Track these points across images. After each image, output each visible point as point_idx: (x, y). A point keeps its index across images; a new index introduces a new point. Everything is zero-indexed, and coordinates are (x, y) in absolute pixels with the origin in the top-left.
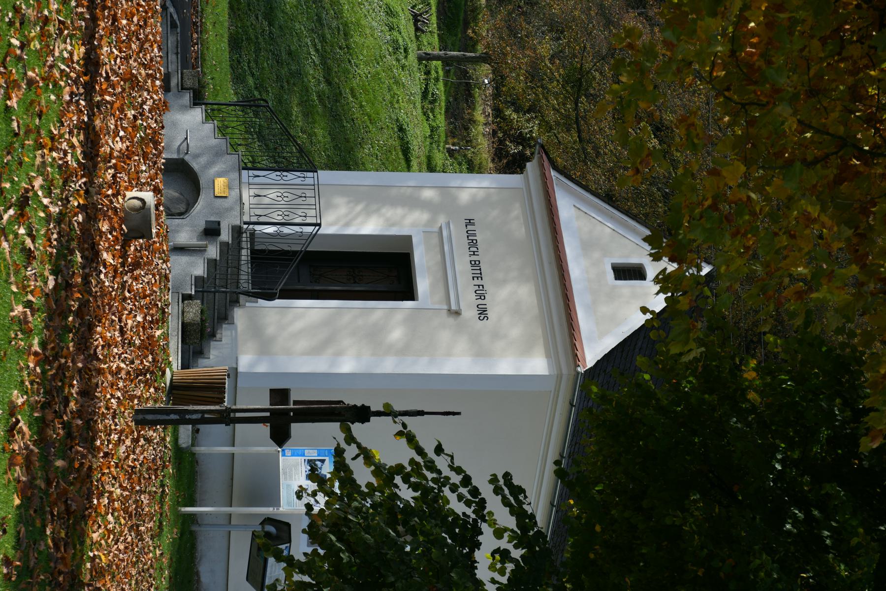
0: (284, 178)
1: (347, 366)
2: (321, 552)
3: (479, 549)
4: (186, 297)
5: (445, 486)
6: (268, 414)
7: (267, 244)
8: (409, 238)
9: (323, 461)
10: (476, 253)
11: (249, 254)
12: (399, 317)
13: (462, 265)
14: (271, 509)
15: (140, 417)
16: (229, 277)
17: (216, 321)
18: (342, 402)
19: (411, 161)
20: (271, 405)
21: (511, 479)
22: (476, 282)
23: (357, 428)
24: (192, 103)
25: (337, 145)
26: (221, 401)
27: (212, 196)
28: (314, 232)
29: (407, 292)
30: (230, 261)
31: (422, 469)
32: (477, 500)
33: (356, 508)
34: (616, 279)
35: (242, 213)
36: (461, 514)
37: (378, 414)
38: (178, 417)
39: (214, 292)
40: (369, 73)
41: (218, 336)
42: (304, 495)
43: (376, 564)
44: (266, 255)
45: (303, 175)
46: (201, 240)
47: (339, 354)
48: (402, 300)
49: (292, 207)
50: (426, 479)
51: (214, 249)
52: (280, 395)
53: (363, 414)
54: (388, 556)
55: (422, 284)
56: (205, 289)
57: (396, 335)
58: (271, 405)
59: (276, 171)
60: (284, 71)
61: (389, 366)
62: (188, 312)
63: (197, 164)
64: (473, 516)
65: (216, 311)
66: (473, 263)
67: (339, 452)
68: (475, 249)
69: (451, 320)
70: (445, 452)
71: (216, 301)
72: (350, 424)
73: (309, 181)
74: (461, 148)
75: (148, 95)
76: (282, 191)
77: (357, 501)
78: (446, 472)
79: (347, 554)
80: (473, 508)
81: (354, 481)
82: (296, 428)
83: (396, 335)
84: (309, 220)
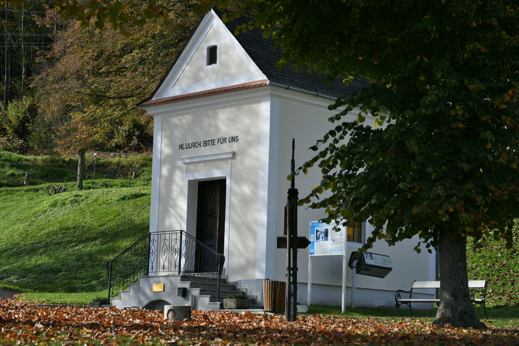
0: (154, 252)
1: (263, 217)
2: (370, 217)
3: (371, 127)
4: (222, 307)
5: (335, 146)
6: (292, 249)
7: (192, 261)
8: (190, 182)
9: (317, 231)
11: (197, 273)
12: (235, 188)
13: (206, 151)
14: (344, 260)
15: (292, 318)
16: (211, 284)
17: (235, 292)
18: (285, 207)
19: (142, 193)
20: (286, 248)
21: (332, 105)
22: (216, 143)
23: (301, 196)
24: (109, 305)
25: (132, 234)
26: (283, 284)
27: (163, 293)
28: (185, 234)
29: (221, 183)
30: (202, 283)
31: (325, 160)
32: (343, 127)
33: (346, 194)
34: (216, 63)
35: (174, 276)
36: (351, 137)
37: (293, 184)
38: (293, 297)
39: (219, 292)
40: (90, 216)
41: (244, 291)
42: (338, 227)
43: (378, 184)
44: (198, 261)
45: (152, 241)
46: (189, 299)
47: (256, 222)
48: (226, 185)
49: (171, 249)
50: (331, 157)
51: (194, 291)
52: (281, 243)
53: (293, 193)
54: (374, 177)
55: (217, 174)
56: (217, 296)
57: (246, 189)
58: (286, 248)
59: (149, 256)
60: (88, 263)
61: (264, 194)
62: (230, 305)
63: (144, 302)
64: (352, 130)
65: (230, 291)
66: (205, 145)
67: (314, 206)
68: (197, 144)
69: (238, 157)
70: (315, 145)
71: (224, 291)
72: (299, 200)
73: (156, 237)
74: (134, 170)
75: (107, 313)
76: (161, 253)
77: (342, 194)
78: (327, 145)
79: (372, 200)
80: (348, 131)
81: (331, 198)
82: (300, 234)
83: (246, 189)
84: (179, 237)
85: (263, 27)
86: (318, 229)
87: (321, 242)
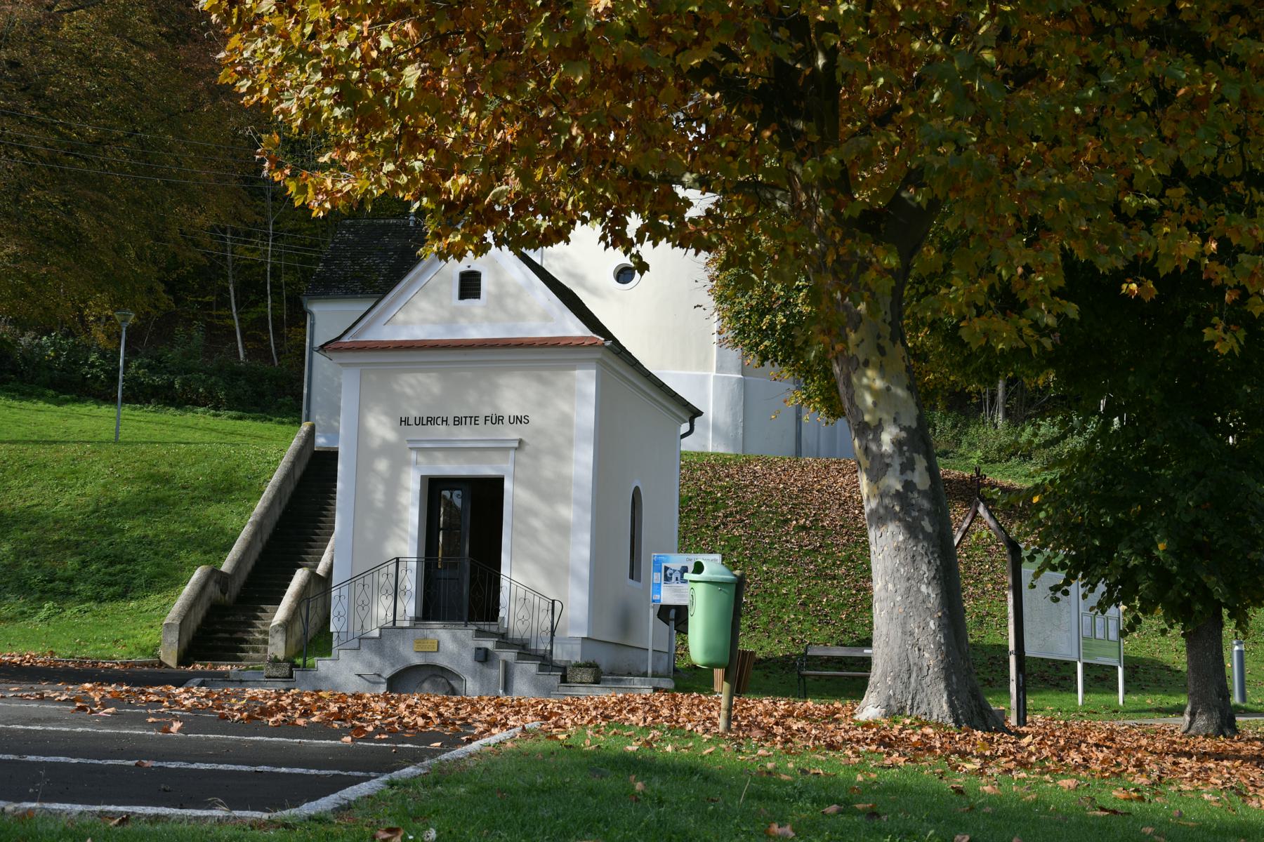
8: (423, 477)
9: (666, 568)
13: (464, 434)
22: (481, 421)
29: (493, 487)
55: (485, 470)
86: (668, 565)
87: (674, 584)
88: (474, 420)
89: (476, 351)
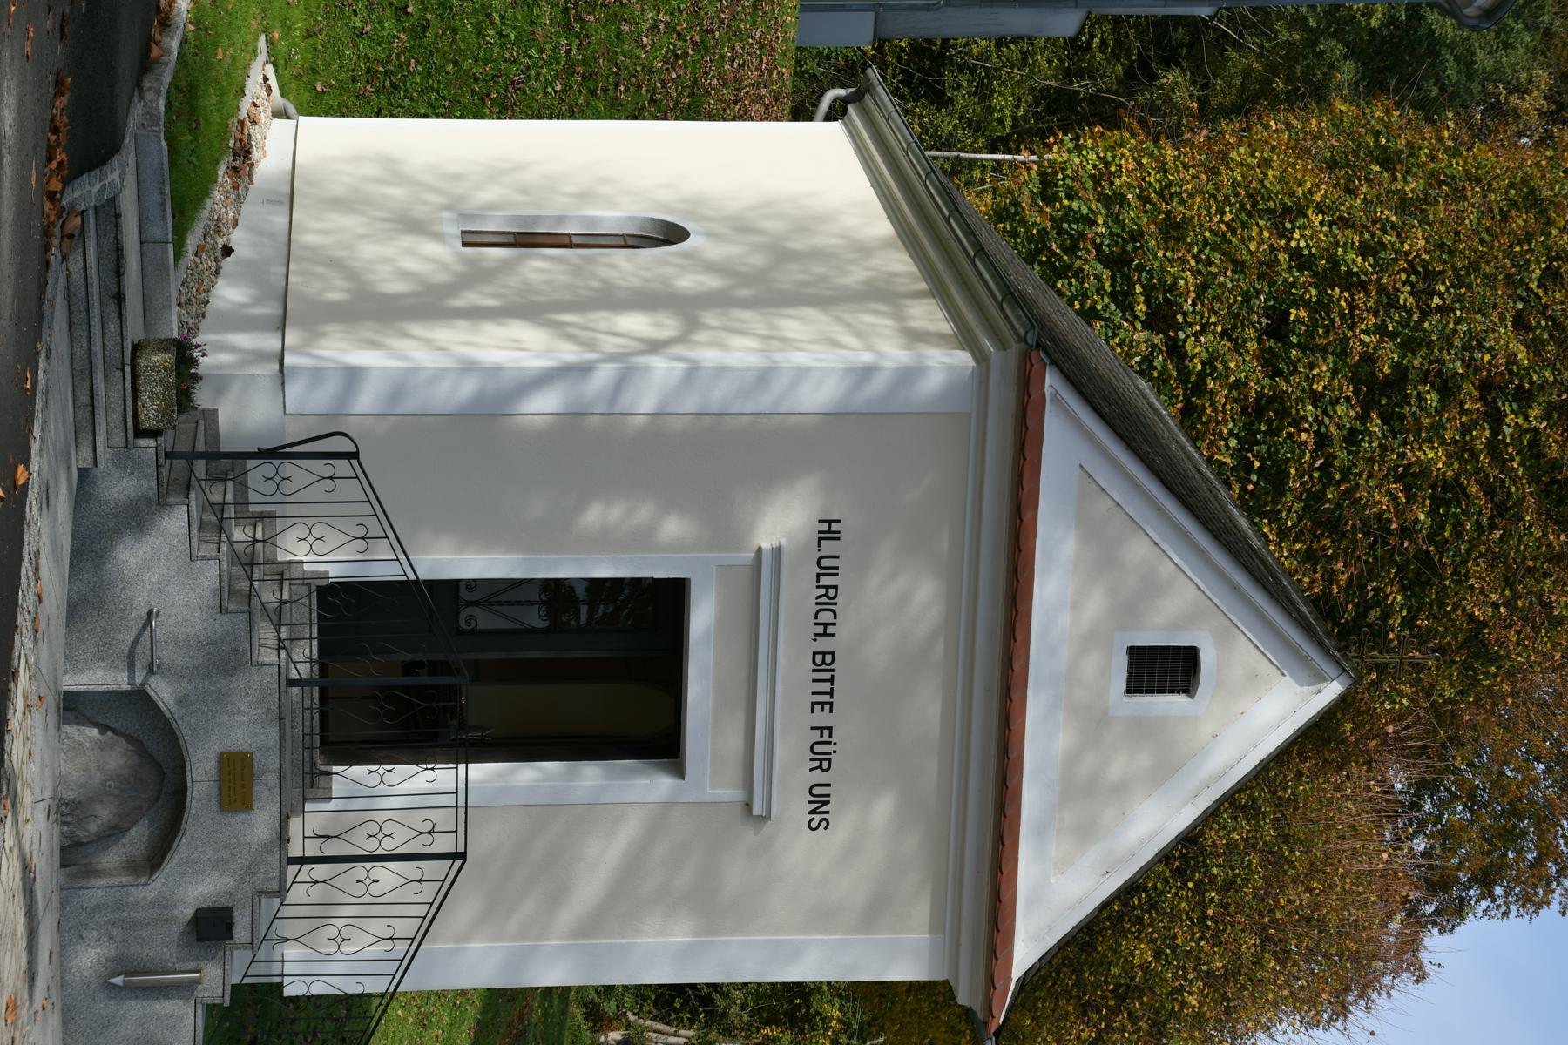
10: (830, 629)
22: (822, 718)
66: (819, 659)
85: (1205, 968)
88: (825, 703)
89: (997, 675)
